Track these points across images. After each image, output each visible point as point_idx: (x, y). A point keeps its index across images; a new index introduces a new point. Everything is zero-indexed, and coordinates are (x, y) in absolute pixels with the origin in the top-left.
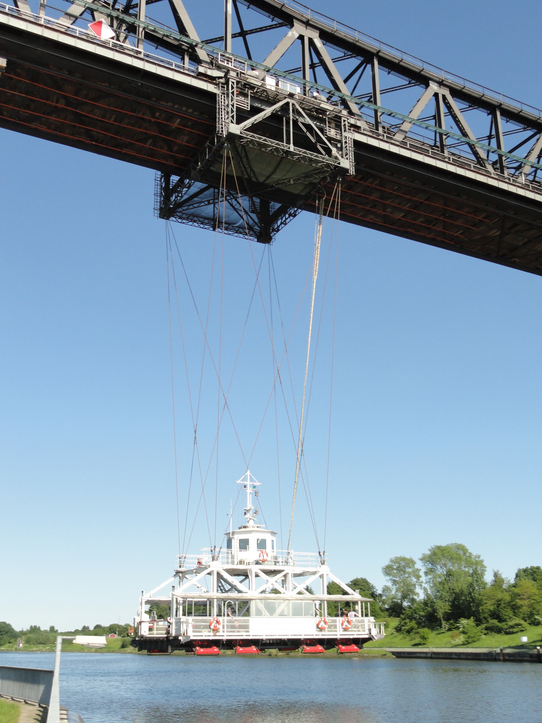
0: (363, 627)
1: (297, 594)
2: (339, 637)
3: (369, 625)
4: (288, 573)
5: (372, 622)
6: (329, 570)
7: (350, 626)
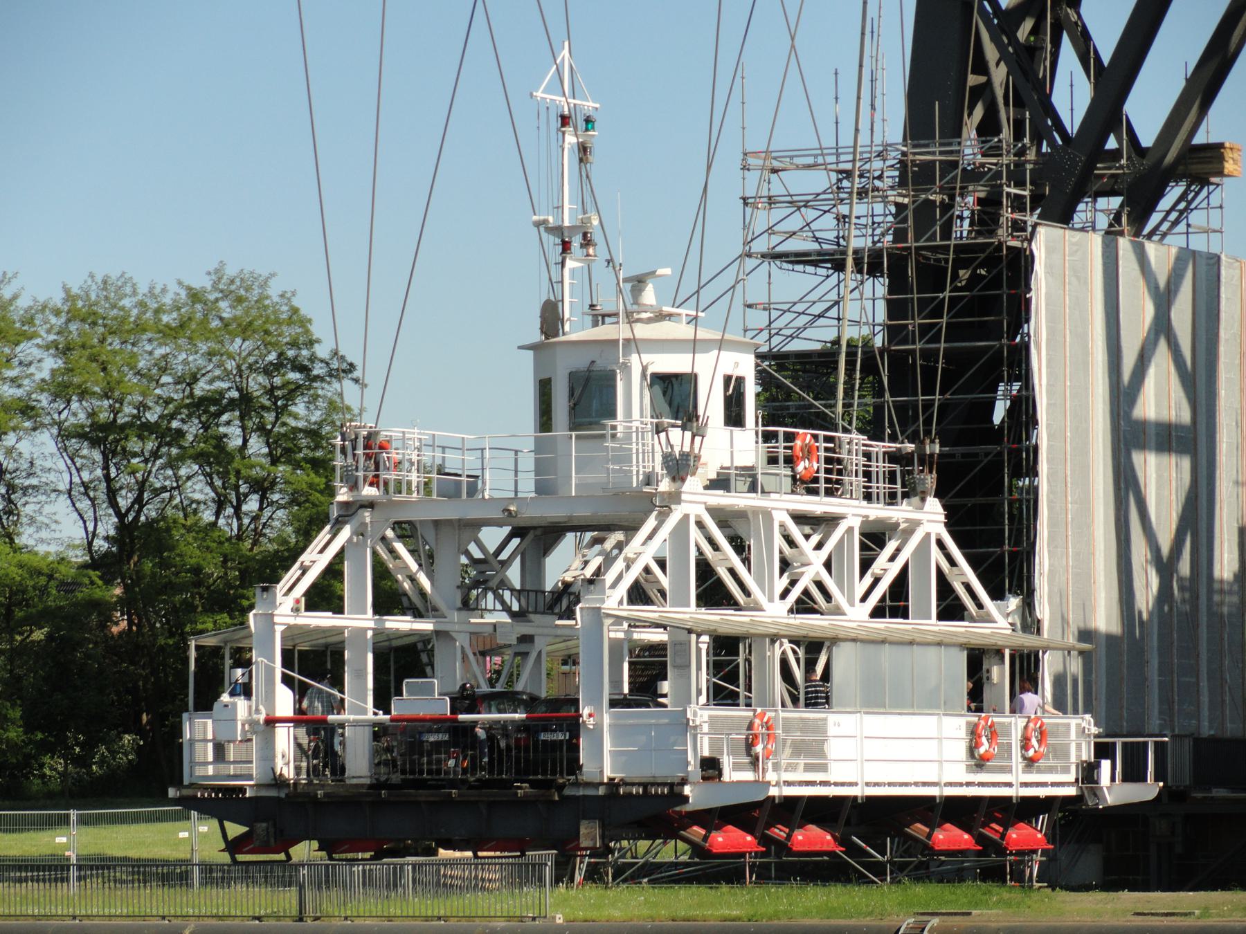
0: (1061, 752)
3: (1079, 747)
5: (1089, 736)
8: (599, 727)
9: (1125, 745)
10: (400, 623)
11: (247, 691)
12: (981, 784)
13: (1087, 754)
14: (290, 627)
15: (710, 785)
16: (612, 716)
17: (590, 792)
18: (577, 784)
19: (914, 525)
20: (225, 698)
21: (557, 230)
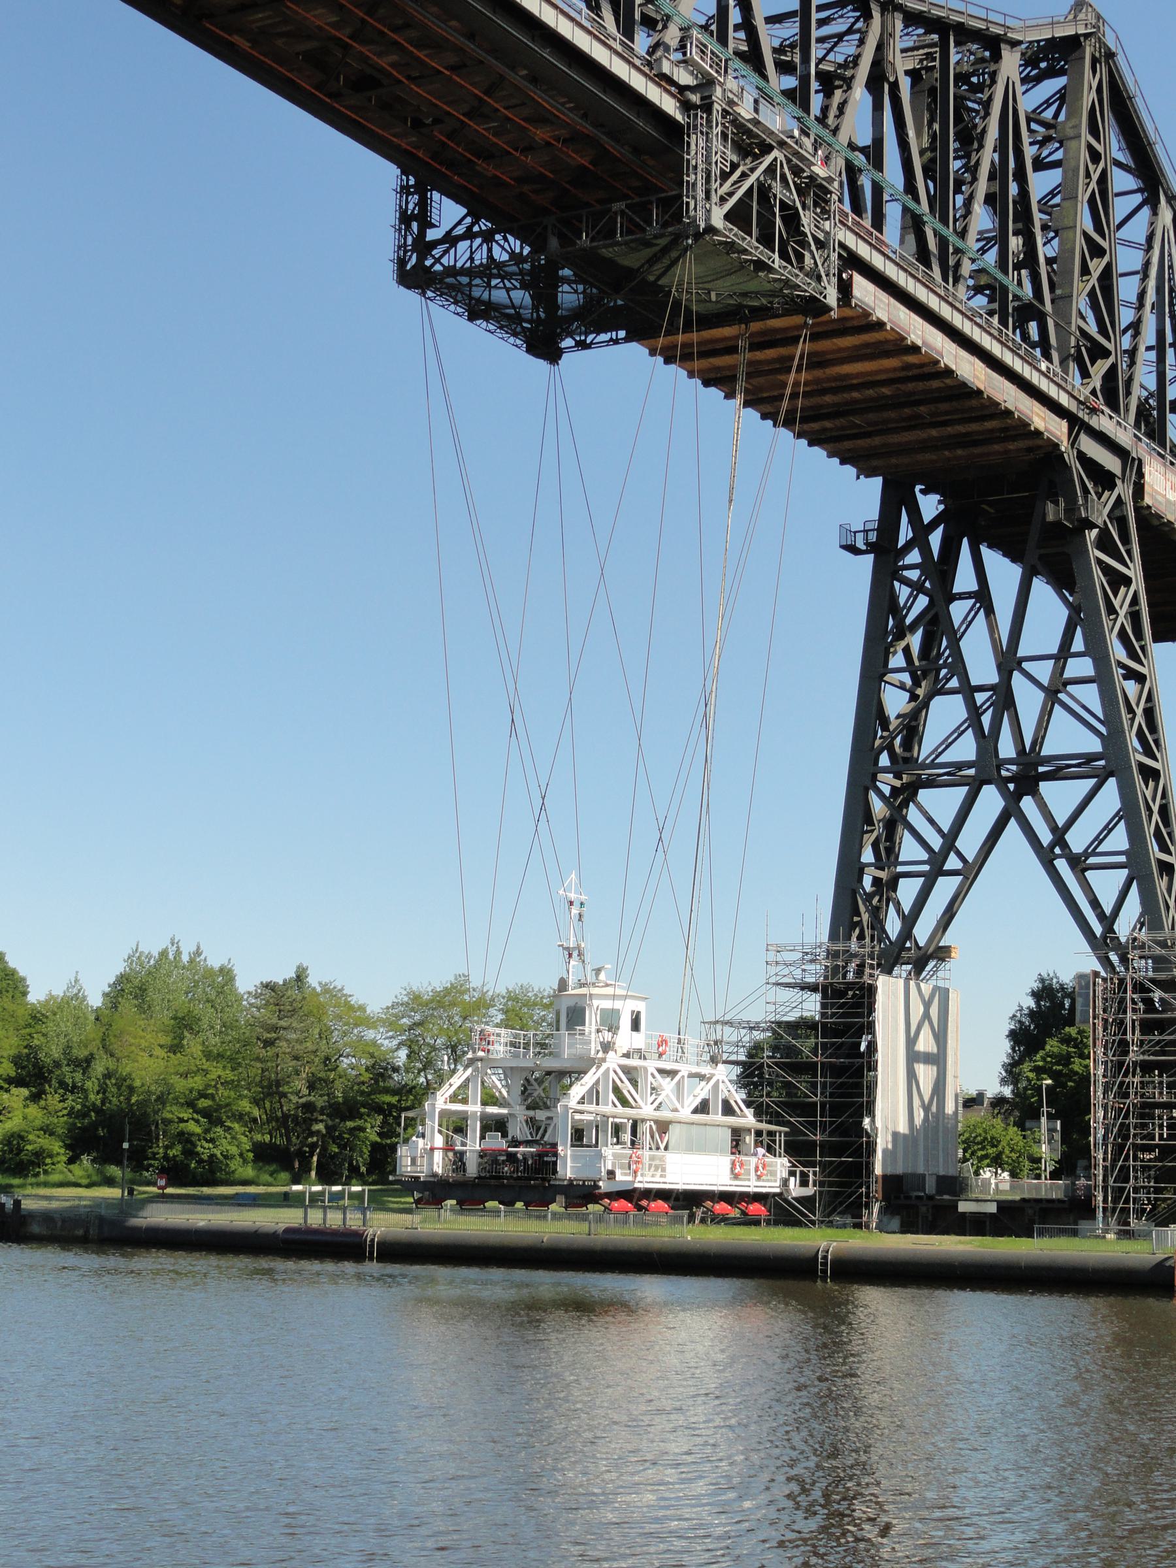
0: (773, 1173)
2: (751, 1190)
3: (781, 1171)
7: (765, 1172)
8: (566, 1155)
10: (493, 1110)
11: (423, 1136)
13: (785, 1174)
14: (442, 1110)
16: (572, 1151)
17: (561, 1183)
18: (556, 1179)
19: (712, 1075)
20: (414, 1138)
21: (568, 949)
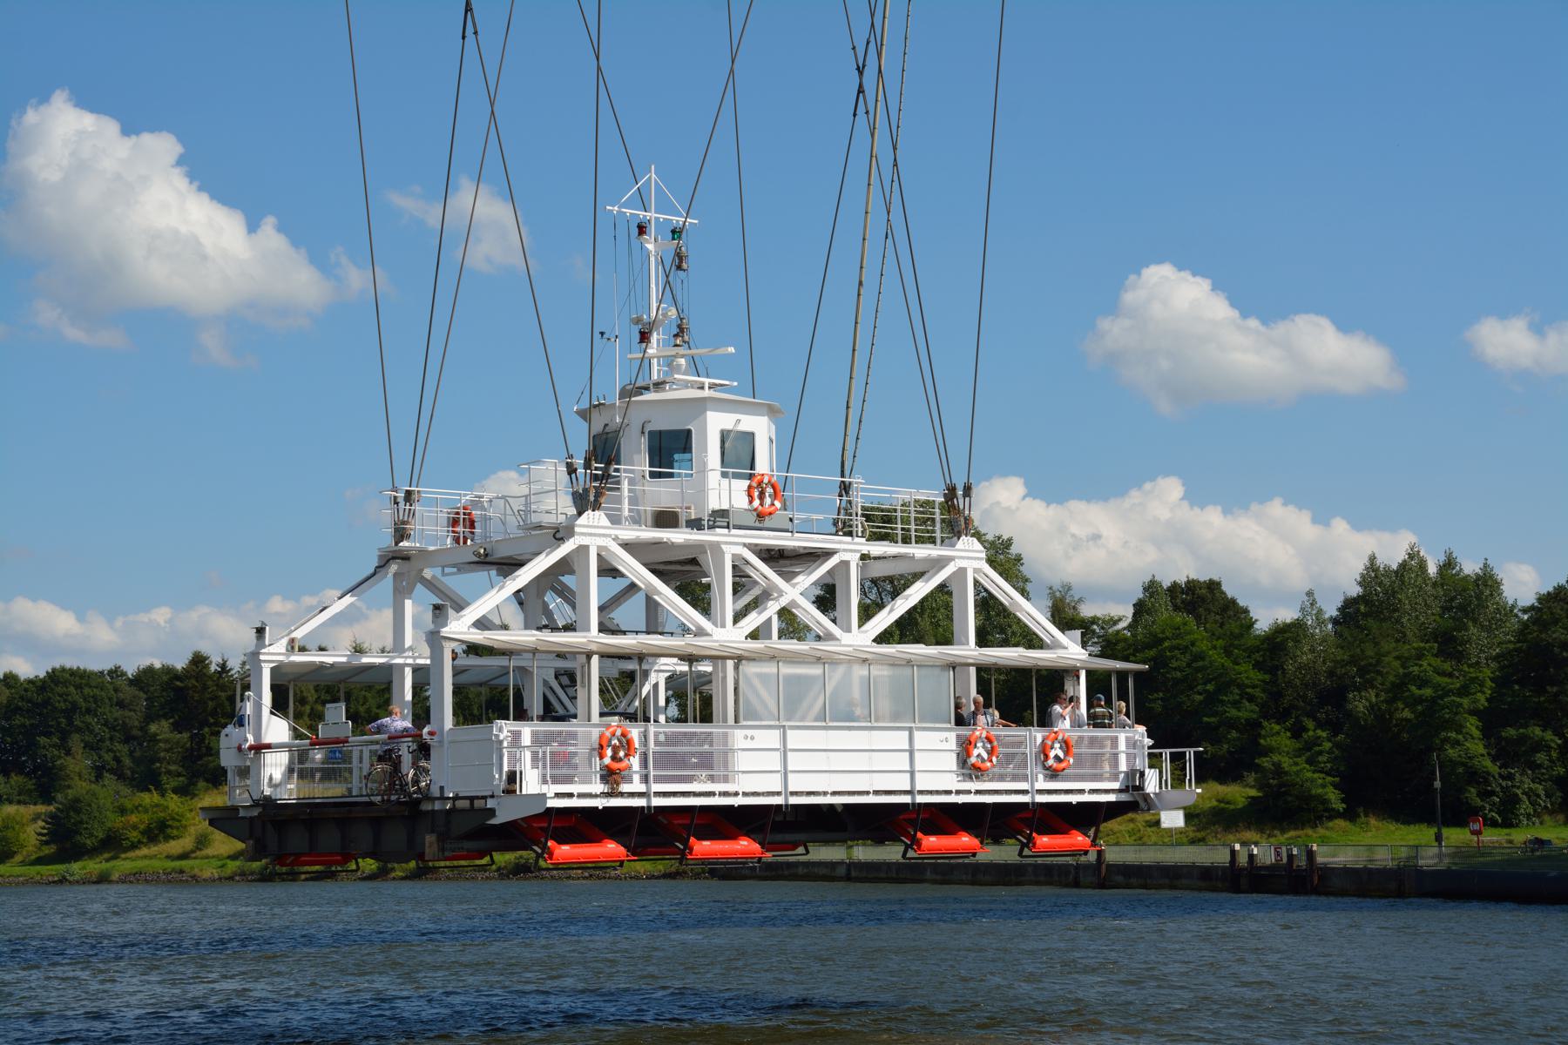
1: (874, 641)
4: (845, 564)
6: (983, 555)
9: (1194, 752)
12: (978, 792)
13: (1141, 763)
15: (510, 798)
